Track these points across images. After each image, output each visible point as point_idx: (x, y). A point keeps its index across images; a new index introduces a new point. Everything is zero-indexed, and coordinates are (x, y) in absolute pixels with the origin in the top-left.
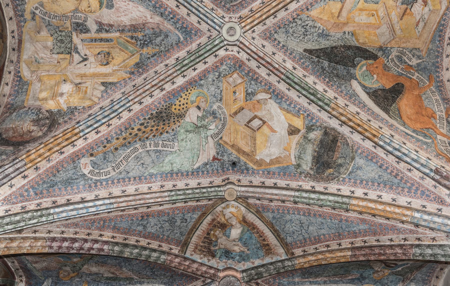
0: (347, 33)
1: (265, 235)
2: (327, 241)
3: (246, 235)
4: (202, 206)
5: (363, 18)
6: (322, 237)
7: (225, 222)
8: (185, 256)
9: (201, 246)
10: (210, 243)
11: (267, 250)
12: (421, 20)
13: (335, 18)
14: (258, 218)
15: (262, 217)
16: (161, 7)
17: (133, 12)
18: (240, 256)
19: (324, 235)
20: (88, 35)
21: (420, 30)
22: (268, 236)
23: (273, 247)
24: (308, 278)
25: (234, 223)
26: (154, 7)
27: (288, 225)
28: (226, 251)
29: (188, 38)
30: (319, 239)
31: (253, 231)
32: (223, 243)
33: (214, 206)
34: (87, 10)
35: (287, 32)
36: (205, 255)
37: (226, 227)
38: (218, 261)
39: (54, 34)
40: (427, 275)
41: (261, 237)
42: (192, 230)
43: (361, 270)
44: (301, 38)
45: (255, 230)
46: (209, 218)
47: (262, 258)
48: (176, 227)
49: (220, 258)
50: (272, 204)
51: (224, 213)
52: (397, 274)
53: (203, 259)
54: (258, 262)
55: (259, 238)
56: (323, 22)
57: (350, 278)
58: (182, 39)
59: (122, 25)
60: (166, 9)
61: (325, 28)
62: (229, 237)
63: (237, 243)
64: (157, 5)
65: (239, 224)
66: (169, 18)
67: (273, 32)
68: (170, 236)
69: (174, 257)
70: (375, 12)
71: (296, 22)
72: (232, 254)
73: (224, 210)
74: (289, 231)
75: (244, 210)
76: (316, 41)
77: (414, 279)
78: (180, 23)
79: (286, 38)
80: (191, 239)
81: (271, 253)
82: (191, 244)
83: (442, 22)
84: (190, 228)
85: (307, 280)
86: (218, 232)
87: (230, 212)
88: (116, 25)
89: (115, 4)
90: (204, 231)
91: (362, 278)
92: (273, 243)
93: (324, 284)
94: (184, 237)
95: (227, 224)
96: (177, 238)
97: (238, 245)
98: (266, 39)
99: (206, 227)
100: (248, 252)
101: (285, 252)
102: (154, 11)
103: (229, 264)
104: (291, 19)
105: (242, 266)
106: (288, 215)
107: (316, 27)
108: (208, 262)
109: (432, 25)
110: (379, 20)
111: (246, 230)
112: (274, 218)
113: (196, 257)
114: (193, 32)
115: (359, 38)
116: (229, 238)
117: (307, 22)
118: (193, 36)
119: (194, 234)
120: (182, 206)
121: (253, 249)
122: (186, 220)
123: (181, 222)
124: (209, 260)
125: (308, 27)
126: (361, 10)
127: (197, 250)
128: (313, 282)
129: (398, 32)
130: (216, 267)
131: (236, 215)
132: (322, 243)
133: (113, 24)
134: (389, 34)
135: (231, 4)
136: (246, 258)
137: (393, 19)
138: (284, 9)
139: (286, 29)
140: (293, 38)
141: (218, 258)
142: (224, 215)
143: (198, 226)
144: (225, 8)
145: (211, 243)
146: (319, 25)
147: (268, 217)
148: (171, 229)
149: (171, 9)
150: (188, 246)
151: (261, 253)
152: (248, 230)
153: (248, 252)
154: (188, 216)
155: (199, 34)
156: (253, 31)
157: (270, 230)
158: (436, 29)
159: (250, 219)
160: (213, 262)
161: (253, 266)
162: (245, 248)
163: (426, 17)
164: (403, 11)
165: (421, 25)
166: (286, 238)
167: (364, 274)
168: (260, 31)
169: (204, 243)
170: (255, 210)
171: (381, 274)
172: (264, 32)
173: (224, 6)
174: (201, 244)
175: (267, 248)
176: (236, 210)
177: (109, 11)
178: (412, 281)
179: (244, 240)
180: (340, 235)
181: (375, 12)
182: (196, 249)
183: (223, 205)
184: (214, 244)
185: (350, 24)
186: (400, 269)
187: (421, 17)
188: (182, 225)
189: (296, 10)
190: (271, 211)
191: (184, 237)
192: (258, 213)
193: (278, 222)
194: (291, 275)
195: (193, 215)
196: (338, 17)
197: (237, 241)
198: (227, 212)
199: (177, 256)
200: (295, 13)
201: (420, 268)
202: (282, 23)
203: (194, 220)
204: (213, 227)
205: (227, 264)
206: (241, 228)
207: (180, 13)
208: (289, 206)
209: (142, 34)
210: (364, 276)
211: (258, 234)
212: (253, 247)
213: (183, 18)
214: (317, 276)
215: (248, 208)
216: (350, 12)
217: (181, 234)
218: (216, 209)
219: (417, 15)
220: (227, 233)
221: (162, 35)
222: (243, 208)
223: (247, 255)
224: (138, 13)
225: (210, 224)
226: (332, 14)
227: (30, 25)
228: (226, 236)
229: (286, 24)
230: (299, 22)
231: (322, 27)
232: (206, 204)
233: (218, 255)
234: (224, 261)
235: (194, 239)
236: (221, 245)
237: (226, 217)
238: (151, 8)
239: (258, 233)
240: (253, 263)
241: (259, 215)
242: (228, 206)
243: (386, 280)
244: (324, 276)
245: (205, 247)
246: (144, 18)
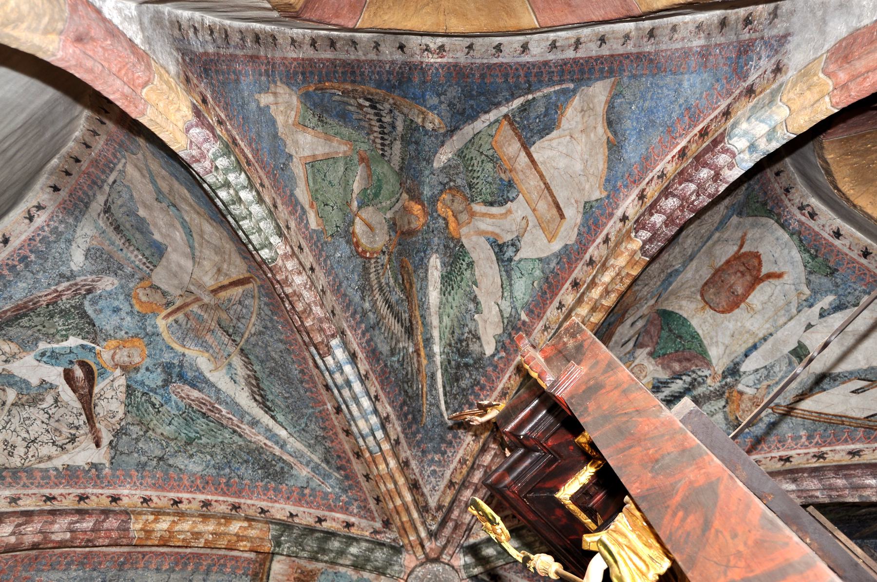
2: (163, 553)
6: (166, 567)
19: (158, 570)
24: (280, 459)
30: (177, 564)
40: (27, 266)
43: (157, 399)
52: (90, 329)
57: (195, 394)
77: (62, 276)
85: (286, 457)
91: (170, 374)
93: (258, 422)
128: (277, 443)
132: (178, 553)
167: (160, 383)
171: (122, 356)
178: (72, 276)
180: (123, 563)
186: (73, 341)
194: (307, 491)
201: (25, 306)
210: (163, 376)
214: (260, 450)
243: (125, 323)
244: (245, 440)
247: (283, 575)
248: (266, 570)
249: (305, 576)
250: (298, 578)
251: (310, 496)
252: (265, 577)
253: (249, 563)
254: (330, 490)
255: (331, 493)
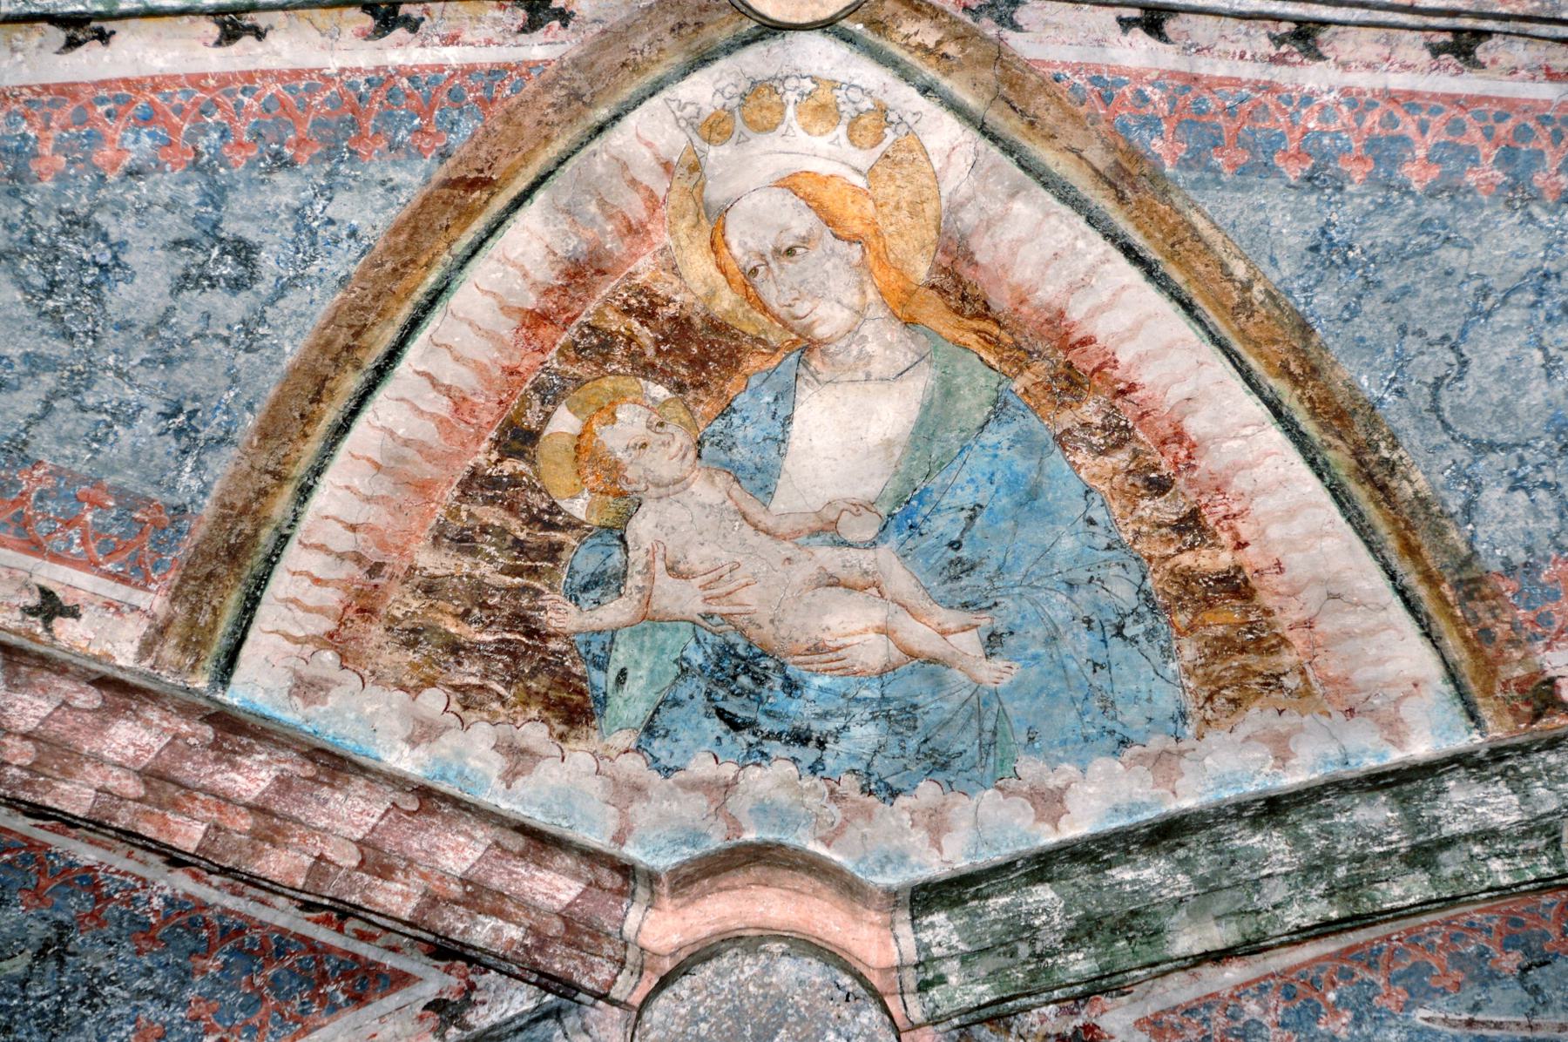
1: (1203, 464)
3: (978, 462)
4: (434, 94)
7: (726, 302)
8: (234, 696)
9: (430, 588)
10: (534, 558)
11: (1224, 646)
14: (1129, 251)
15: (1182, 238)
18: (899, 716)
22: (1240, 483)
23: (1294, 615)
25: (828, 318)
27: (1494, 349)
28: (727, 650)
31: (1067, 419)
32: (696, 558)
33: (588, 100)
36: (468, 698)
37: (731, 361)
38: (634, 765)
41: (1160, 487)
42: (313, 384)
45: (1090, 410)
46: (529, 245)
47: (1156, 743)
48: (113, 339)
49: (649, 730)
50: (1313, 77)
51: (715, 193)
53: (450, 741)
54: (1098, 799)
55: (1133, 499)
62: (760, 479)
63: (864, 558)
65: (895, 333)
68: (43, 442)
69: (89, 698)
72: (791, 687)
73: (715, 154)
74: (1505, 411)
75: (962, 162)
80: (305, 492)
81: (1273, 681)
82: (294, 556)
84: (291, 353)
86: (630, 422)
87: (789, 183)
90: (460, 403)
92: (1298, 564)
94: (222, 466)
95: (750, 323)
96: (129, 479)
97: (870, 585)
99: (484, 352)
100: (992, 672)
101: (1452, 675)
103: (763, 810)
105: (919, 837)
106: (1507, 221)
108: (510, 777)
111: (972, 404)
112: (1325, 251)
113: (373, 719)
116: (766, 492)
119: (342, 429)
120: (197, 80)
121: (1052, 640)
122: (243, 252)
123: (184, 281)
124: (519, 758)
127: (376, 631)
130: (597, 839)
131: (855, 215)
136: (966, 742)
141: (623, 739)
142: (714, 221)
143: (390, 334)
145: (553, 552)
147: (1259, 232)
148: (51, 365)
150: (262, 581)
151: (1155, 679)
152: (999, 408)
153: (992, 672)
154: (262, 208)
157: (1276, 409)
159: (1023, 272)
160: (567, 784)
161: (1048, 838)
162: (953, 619)
166: (1469, 509)
169: (465, 542)
170: (1098, 156)
174: (432, 561)
175: (1226, 617)
176: (863, 159)
179: (945, 525)
182: (366, 612)
183: (703, 90)
184: (585, 561)
188: (186, 321)
190: (1294, 171)
191: (222, 466)
192: (1134, 202)
193: (1373, 304)
194: (1512, 960)
195: (328, 191)
197: (863, 529)
198: (749, 173)
199: (120, 692)
203: (341, 262)
204: (575, 351)
205: (739, 804)
206: (919, 385)
208: (1530, 107)
211: (1121, 458)
212: (1059, 607)
215: (1009, 125)
217: (182, 421)
218: (619, 139)
220: (748, 432)
222: (944, 135)
223: (981, 704)
225: (539, 318)
228: (735, 472)
232: (497, 72)
233: (631, 704)
234: (702, 766)
235: (342, 498)
236: (664, 581)
237: (742, 241)
239: (1118, 436)
240: (1049, 803)
241: (1147, 217)
242: (757, 107)
245: (478, 592)
247: (1348, 635)
248: (1441, 624)
249: (1246, 671)
250: (1272, 650)
251: (1482, 953)
252: (1422, 591)
253: (1543, 620)
254: (1419, 1015)
255: (1407, 1007)
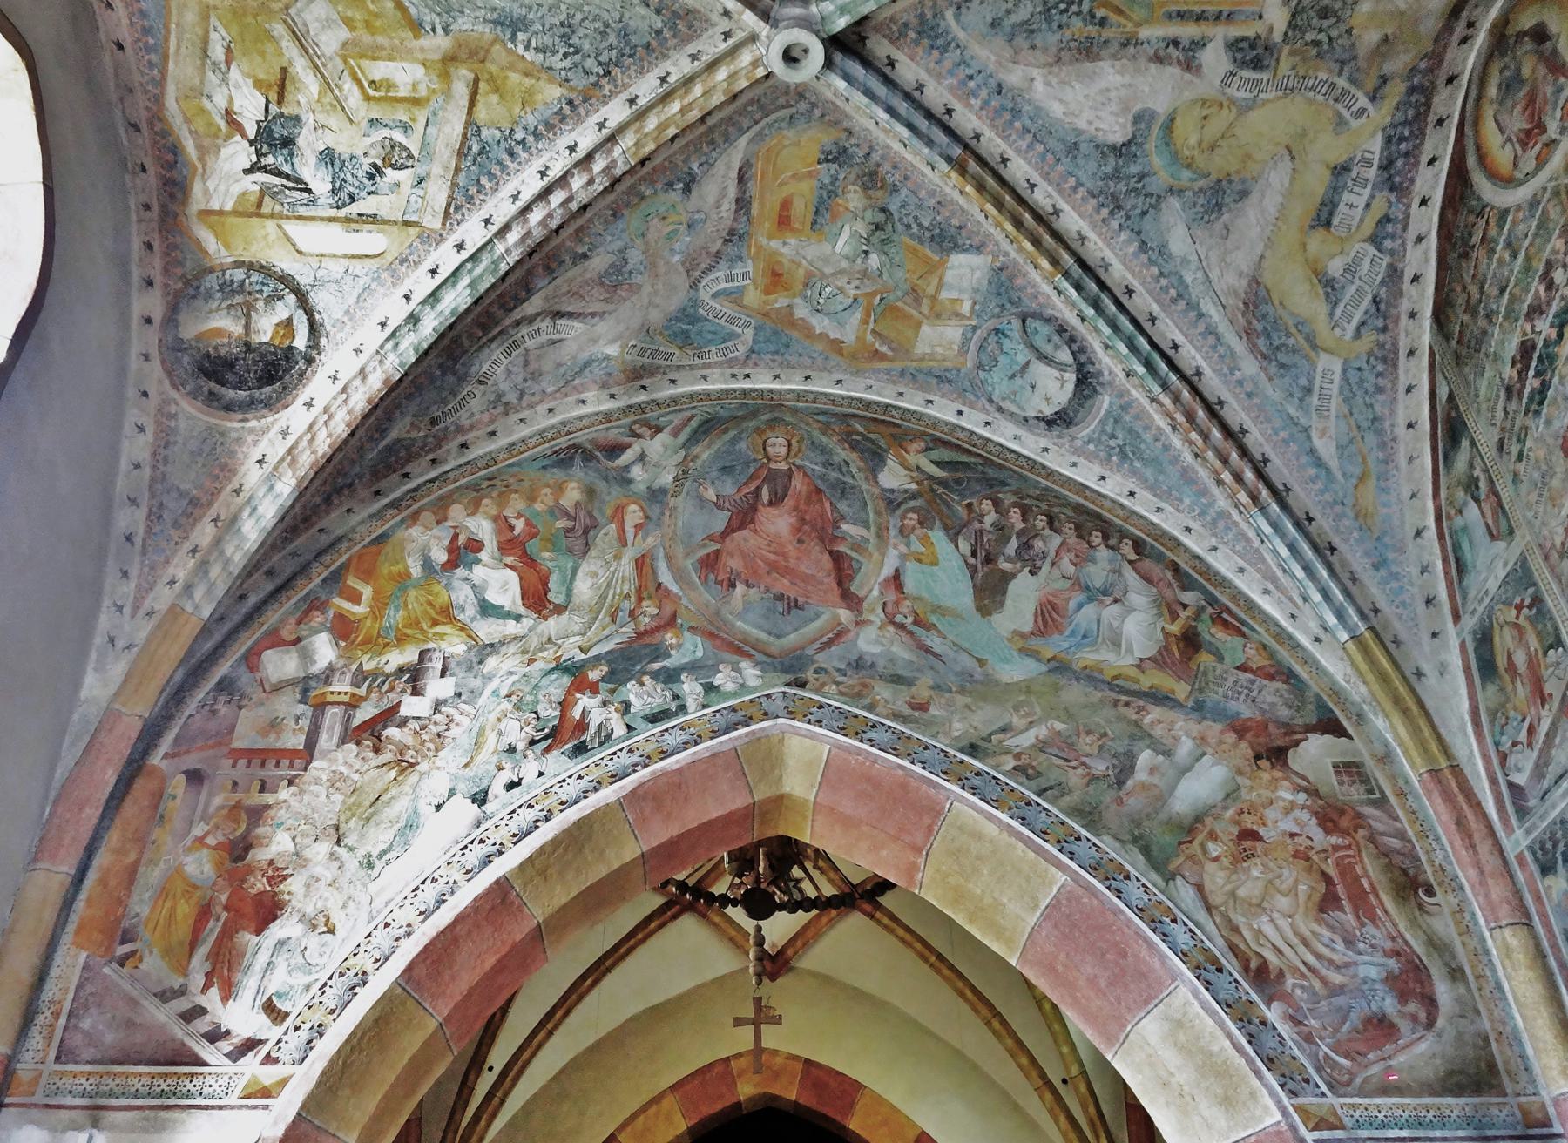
0: (439, 30)
5: (405, 75)
12: (223, 67)
13: (486, 76)
16: (998, 112)
17: (1081, 99)
20: (1235, 31)
21: (213, 36)
26: (1016, 113)
29: (929, 15)
34: (1214, 109)
35: (625, 34)
39: (1340, 36)
44: (579, 16)
56: (521, 65)
58: (949, 14)
59: (1124, 61)
60: (985, 104)
61: (510, 45)
64: (1007, 116)
66: (979, 79)
67: (667, 33)
70: (372, 92)
71: (600, 64)
76: (530, 8)
78: (947, 64)
79: (627, 15)
83: (154, 57)
88: (1142, 62)
89: (1129, 125)
98: (688, 12)
102: (1019, 100)
104: (616, 72)
107: (537, 49)
109: (183, 49)
110: (352, 68)
114: (912, 35)
115: (399, 14)
117: (567, 63)
118: (914, 21)
125: (562, 51)
126: (416, 102)
129: (279, 29)
133: (1153, 66)
134: (305, 25)
135: (794, 110)
137: (312, 76)
138: (642, 102)
139: (628, 43)
140: (606, 16)
144: (813, 99)
146: (529, 56)
149: (968, 105)
155: (895, 29)
156: (727, 35)
158: (167, 40)
163: (213, 78)
164: (288, 97)
165: (218, 52)
168: (705, 35)
172: (693, 35)
173: (814, 105)
177: (1150, 105)
181: (372, 92)
185: (437, 57)
187: (225, 74)
189: (605, 100)
196: (476, 81)
200: (606, 92)
202: (641, 60)
207: (945, 92)
209: (1068, 34)
213: (939, 77)
216: (447, 94)
219: (241, 82)
221: (1008, 29)
224: (1069, 94)
226: (497, 90)
227: (1398, 63)
229: (630, 56)
230: (590, 63)
231: (520, 49)
238: (1027, 108)
246: (1054, 81)
